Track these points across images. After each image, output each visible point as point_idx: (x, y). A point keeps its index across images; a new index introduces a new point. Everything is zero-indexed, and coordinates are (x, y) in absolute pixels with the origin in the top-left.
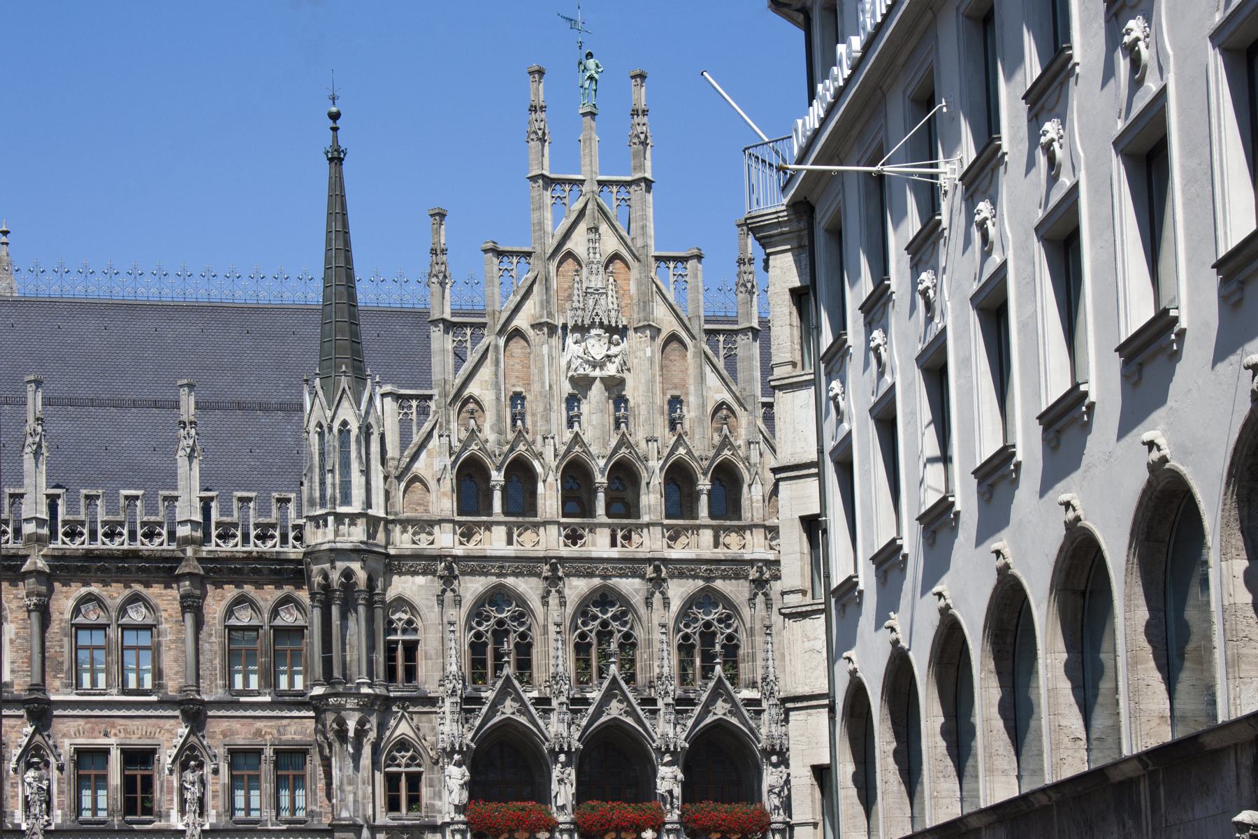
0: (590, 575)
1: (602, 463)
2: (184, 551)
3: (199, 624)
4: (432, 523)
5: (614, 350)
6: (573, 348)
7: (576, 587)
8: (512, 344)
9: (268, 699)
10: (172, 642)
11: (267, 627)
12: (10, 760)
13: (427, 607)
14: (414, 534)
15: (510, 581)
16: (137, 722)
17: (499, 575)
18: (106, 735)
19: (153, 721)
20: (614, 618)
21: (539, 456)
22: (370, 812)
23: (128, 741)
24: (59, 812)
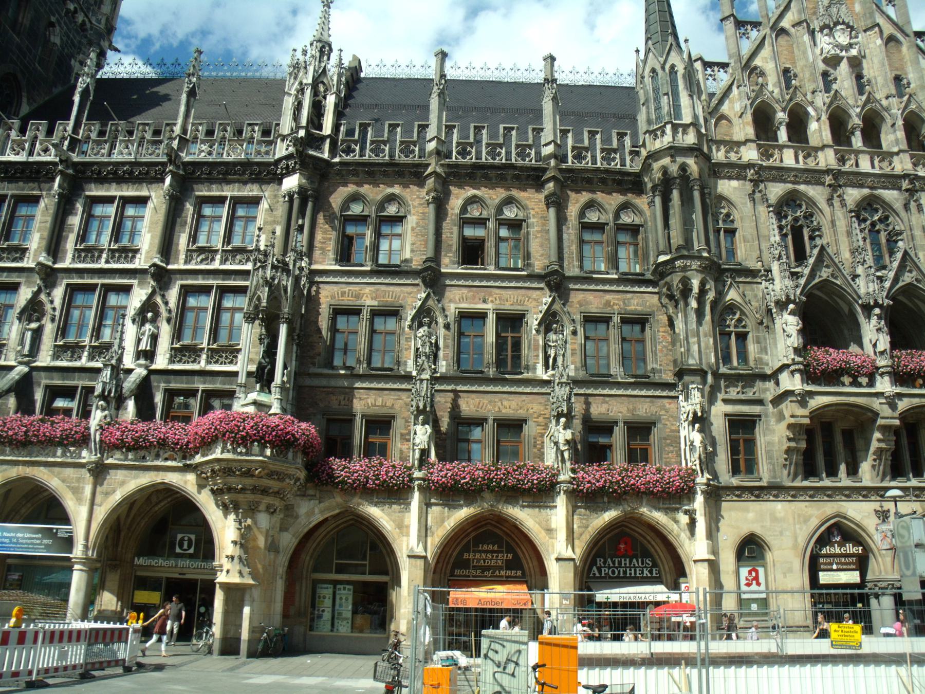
0: (861, 186)
1: (858, 110)
2: (549, 164)
3: (561, 220)
4: (739, 144)
5: (853, 41)
6: (823, 41)
7: (852, 195)
8: (779, 39)
9: (616, 277)
10: (538, 232)
11: (612, 224)
12: (406, 320)
13: (742, 204)
14: (727, 152)
15: (802, 188)
16: (510, 292)
17: (794, 183)
18: (485, 301)
19: (523, 291)
20: (880, 220)
21: (811, 103)
22: (713, 360)
23: (502, 307)
24: (444, 363)
